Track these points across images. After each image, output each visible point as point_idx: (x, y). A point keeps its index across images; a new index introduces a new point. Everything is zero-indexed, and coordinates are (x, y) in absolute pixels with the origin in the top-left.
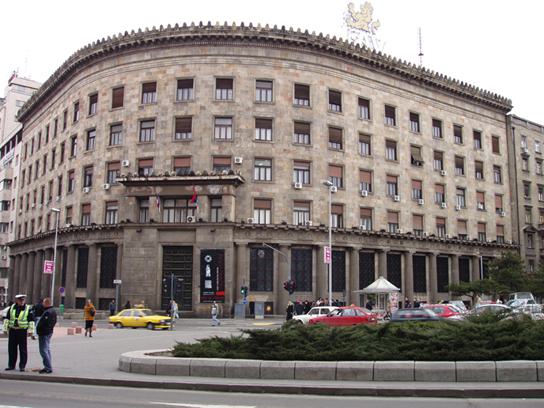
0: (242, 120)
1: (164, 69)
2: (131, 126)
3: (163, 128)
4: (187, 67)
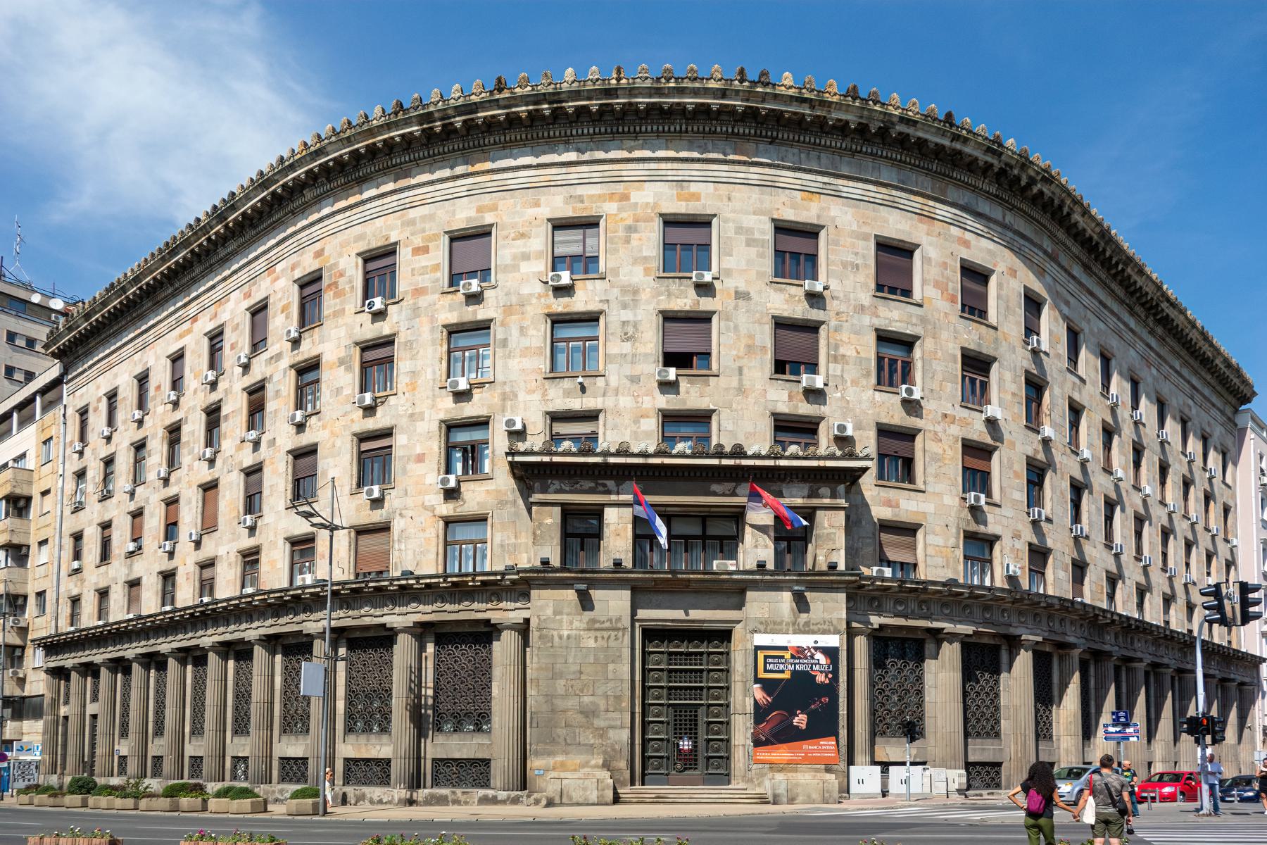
0: (844, 336)
1: (620, 188)
2: (523, 331)
3: (627, 338)
4: (694, 188)
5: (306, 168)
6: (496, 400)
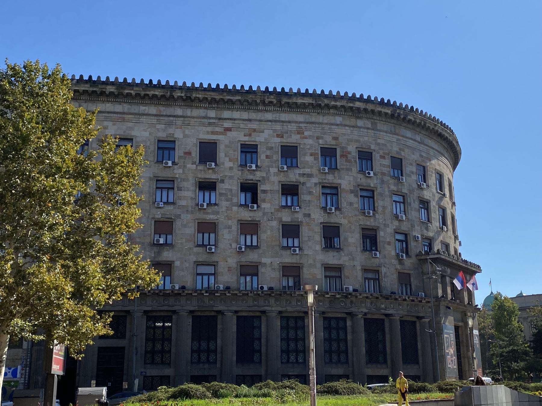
5: (342, 104)
6: (410, 226)
